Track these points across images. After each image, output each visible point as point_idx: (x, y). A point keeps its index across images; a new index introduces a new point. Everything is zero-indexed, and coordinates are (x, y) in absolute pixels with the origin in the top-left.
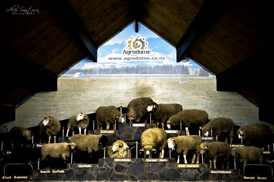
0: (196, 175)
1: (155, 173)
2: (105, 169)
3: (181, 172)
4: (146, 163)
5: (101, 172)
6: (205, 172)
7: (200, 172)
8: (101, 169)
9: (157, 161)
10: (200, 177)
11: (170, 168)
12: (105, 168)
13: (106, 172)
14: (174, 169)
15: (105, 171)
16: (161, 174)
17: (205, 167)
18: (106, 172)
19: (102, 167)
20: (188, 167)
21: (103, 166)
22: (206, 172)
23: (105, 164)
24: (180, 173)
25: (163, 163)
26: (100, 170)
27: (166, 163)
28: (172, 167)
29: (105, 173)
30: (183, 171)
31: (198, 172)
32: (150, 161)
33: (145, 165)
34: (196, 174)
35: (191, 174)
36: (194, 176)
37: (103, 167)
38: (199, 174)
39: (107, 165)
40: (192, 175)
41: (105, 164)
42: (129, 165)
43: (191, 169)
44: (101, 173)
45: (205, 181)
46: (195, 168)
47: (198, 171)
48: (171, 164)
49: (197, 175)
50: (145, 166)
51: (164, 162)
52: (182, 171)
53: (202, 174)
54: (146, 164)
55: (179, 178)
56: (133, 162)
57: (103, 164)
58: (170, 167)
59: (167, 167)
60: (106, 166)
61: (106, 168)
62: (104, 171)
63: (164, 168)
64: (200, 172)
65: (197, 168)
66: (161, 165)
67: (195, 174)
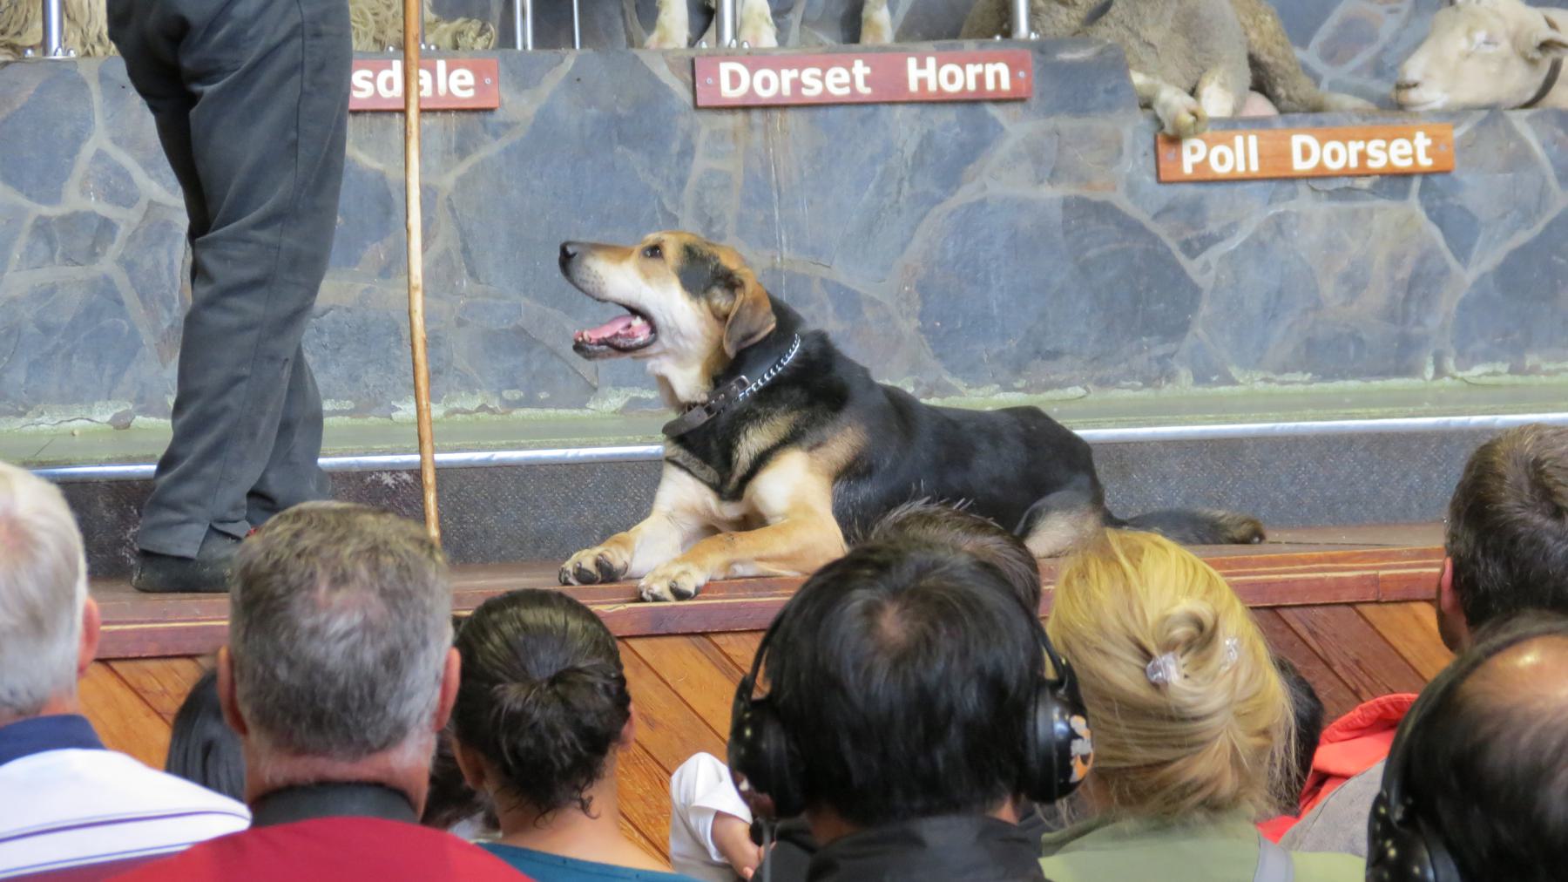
0: (1412, 284)
1: (844, 274)
2: (107, 227)
3: (1208, 241)
4: (708, 124)
5: (45, 276)
6: (1523, 237)
7: (1461, 231)
8: (42, 228)
9: (864, 90)
10: (1464, 307)
11: (1052, 193)
12: (104, 209)
13: (121, 280)
14: (1104, 211)
15: (107, 264)
16: (923, 289)
17: (1520, 159)
18: (121, 280)
19: (54, 198)
20: (1299, 165)
21: (63, 176)
22: (1539, 227)
23: (100, 156)
24: (1192, 267)
25: (950, 114)
26: (23, 240)
27: (993, 111)
28: (1082, 180)
29: (107, 292)
30: (1232, 227)
31: (1436, 232)
32: (766, 95)
33: (687, 152)
34: (1403, 274)
35: (1343, 265)
36: (1376, 297)
37: (78, 198)
38: (1446, 271)
39: (127, 160)
40: (1354, 283)
41: (100, 156)
42: (462, 151)
43: (1333, 195)
44: (48, 292)
45: (1531, 360)
46: (1395, 181)
47: (1438, 218)
48: (1066, 123)
49: (1420, 283)
50: (700, 164)
51: (971, 102)
52: (1212, 227)
53: (1487, 258)
54: (701, 139)
55: (1177, 330)
56: (519, 107)
57: (73, 152)
58: (1053, 177)
59: (1008, 180)
60: (125, 176)
61: (126, 219)
62: (92, 255)
63: (965, 195)
64: (1461, 231)
65: (1426, 174)
66: (927, 141)
67: (1395, 261)
